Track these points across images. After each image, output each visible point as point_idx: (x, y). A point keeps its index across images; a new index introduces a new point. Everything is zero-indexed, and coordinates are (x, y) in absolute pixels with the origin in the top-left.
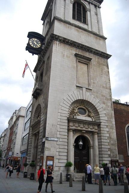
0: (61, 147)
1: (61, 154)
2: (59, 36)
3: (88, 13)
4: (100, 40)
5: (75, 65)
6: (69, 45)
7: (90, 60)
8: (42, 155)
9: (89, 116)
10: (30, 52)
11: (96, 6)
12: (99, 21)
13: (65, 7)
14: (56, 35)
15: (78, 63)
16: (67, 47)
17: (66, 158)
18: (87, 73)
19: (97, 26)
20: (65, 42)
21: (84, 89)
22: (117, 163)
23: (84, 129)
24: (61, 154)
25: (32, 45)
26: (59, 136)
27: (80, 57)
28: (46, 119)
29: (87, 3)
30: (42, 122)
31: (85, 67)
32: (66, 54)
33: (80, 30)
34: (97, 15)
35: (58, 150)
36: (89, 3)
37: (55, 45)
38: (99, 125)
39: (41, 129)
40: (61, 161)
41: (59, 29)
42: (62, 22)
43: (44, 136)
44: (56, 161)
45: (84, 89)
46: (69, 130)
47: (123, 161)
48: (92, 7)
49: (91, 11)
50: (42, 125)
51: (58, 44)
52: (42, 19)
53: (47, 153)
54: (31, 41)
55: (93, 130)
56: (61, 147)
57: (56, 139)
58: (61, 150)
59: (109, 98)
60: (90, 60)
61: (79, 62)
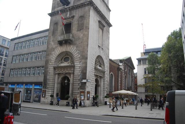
7: (104, 26)
9: (100, 66)
15: (100, 28)
18: (102, 36)
20: (96, 10)
21: (101, 48)
23: (99, 75)
26: (91, 79)
27: (101, 24)
31: (101, 31)
32: (95, 19)
35: (91, 88)
38: (104, 72)
45: (101, 48)
55: (102, 76)
57: (90, 81)
59: (108, 55)
60: (104, 26)
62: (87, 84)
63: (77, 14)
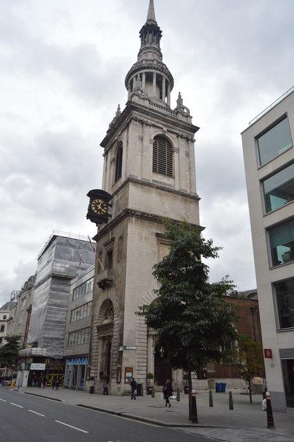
0: (141, 356)
1: (140, 364)
2: (135, 211)
3: (175, 155)
4: (190, 202)
5: (156, 250)
6: (148, 220)
8: (119, 366)
10: (92, 221)
11: (188, 140)
12: (191, 168)
13: (142, 152)
16: (147, 223)
17: (145, 368)
19: (188, 177)
20: (144, 217)
22: (205, 375)
24: (140, 364)
25: (96, 211)
26: (137, 344)
28: (123, 323)
29: (174, 136)
30: (116, 326)
32: (144, 235)
33: (164, 192)
34: (188, 155)
36: (178, 136)
37: (131, 223)
39: (116, 334)
40: (142, 372)
41: (137, 199)
42: (139, 185)
43: (121, 344)
44: (135, 372)
46: (148, 336)
47: (214, 371)
48: (182, 142)
50: (117, 330)
52: (103, 145)
53: (125, 364)
56: (141, 356)
58: (141, 360)
61: (161, 243)
62: (124, 355)
63: (117, 233)
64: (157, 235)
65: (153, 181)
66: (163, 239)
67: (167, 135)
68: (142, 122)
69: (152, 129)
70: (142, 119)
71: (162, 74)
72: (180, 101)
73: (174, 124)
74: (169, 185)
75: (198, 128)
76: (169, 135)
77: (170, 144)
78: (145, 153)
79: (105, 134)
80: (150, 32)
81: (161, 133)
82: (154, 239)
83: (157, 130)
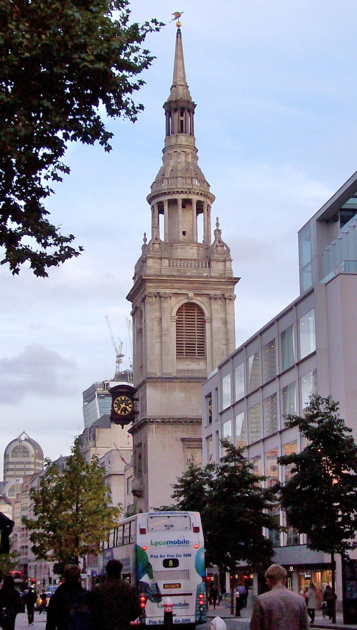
3: (207, 325)
13: (161, 337)
14: (149, 419)
16: (169, 427)
25: (119, 412)
29: (205, 299)
34: (225, 322)
36: (210, 298)
37: (151, 432)
48: (217, 306)
49: (213, 321)
51: (154, 430)
54: (116, 403)
64: (183, 440)
65: (178, 371)
66: (191, 443)
67: (194, 301)
68: (159, 296)
69: (174, 300)
70: (159, 290)
71: (190, 197)
72: (218, 232)
73: (203, 283)
74: (199, 371)
75: (239, 279)
76: (197, 301)
77: (201, 312)
78: (164, 339)
79: (132, 284)
80: (176, 110)
81: (186, 301)
82: (180, 444)
83: (181, 298)
